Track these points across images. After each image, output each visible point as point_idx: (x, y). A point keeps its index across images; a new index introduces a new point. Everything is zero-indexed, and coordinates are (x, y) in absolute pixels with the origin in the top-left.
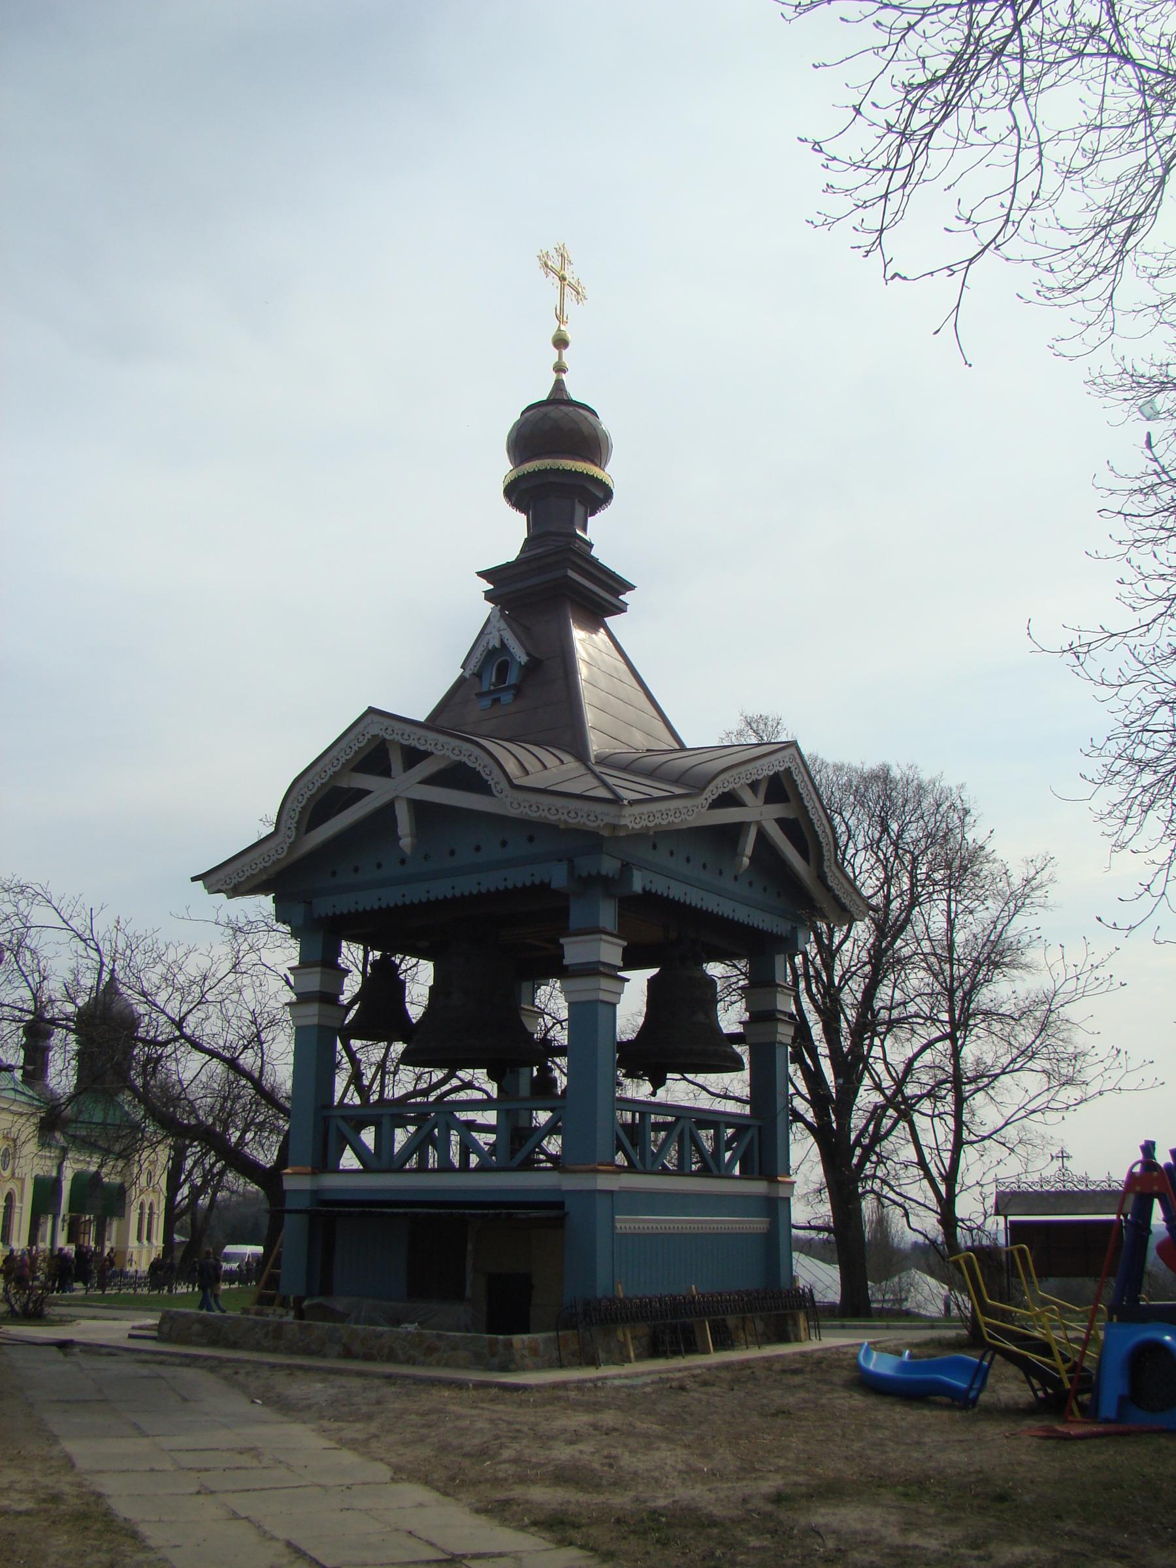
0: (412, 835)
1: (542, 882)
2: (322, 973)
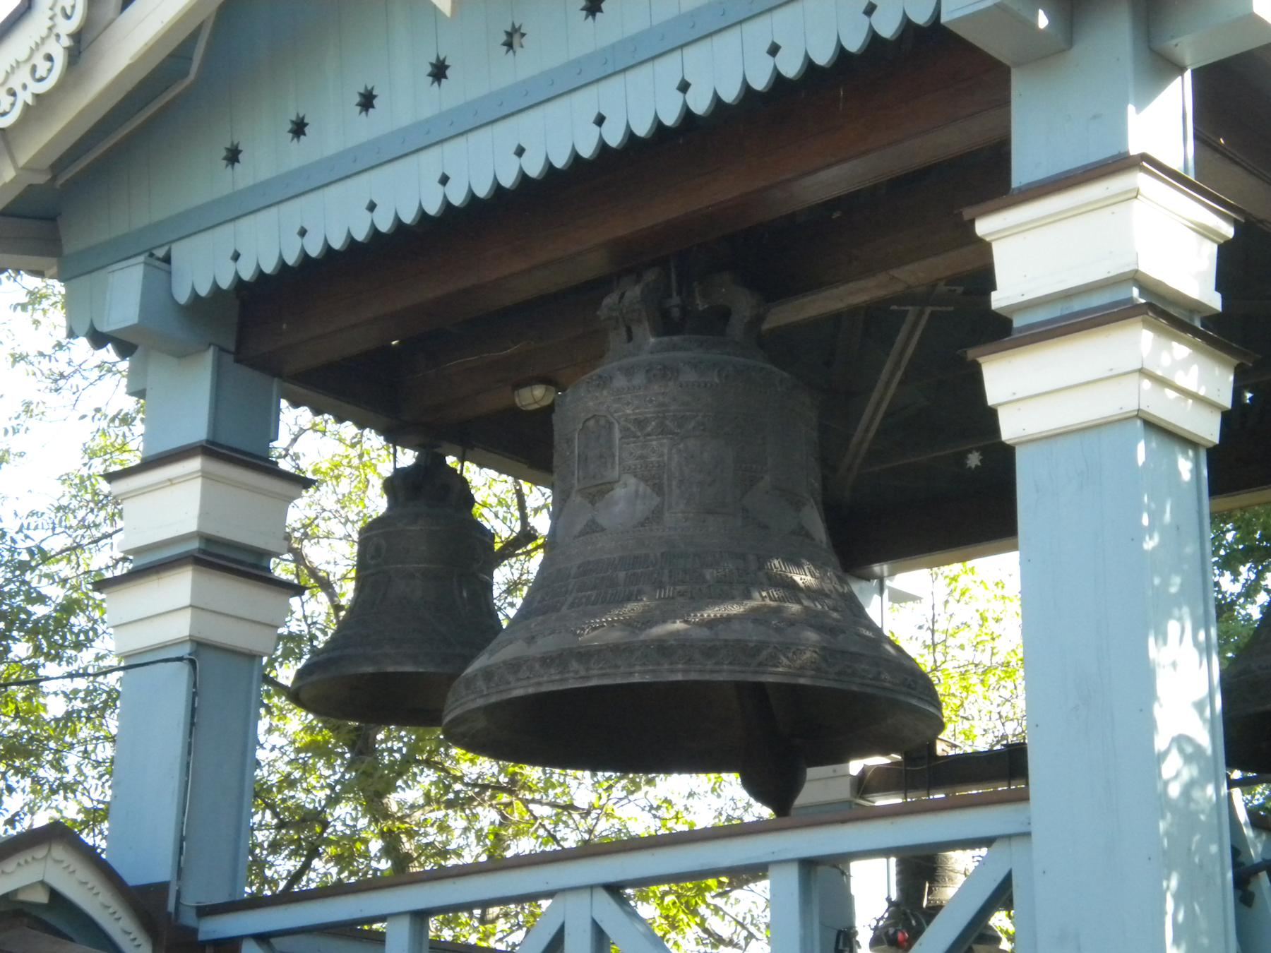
1: (908, 26)
2: (205, 475)
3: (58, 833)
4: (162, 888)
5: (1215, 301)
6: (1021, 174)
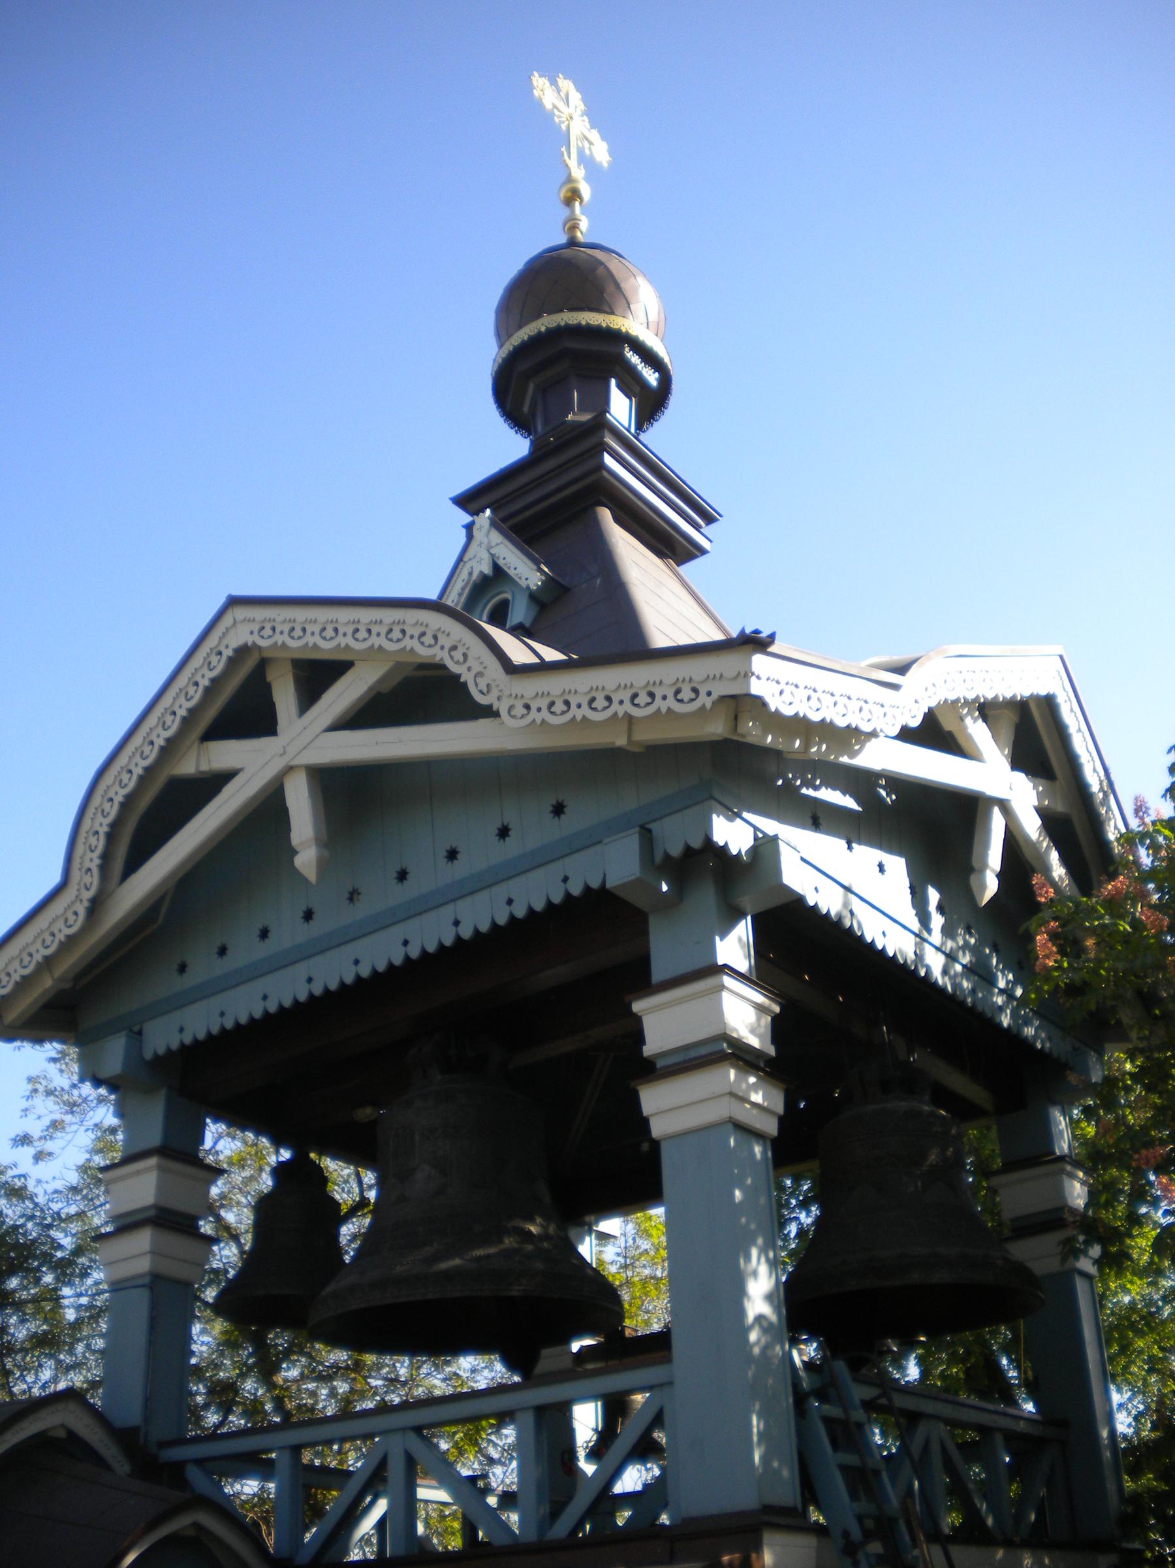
0: (319, 842)
1: (588, 889)
2: (159, 1168)
3: (71, 1394)
4: (135, 1430)
5: (771, 1051)
6: (659, 973)
